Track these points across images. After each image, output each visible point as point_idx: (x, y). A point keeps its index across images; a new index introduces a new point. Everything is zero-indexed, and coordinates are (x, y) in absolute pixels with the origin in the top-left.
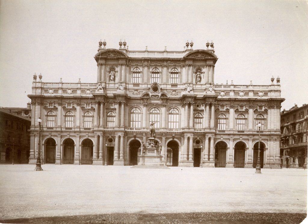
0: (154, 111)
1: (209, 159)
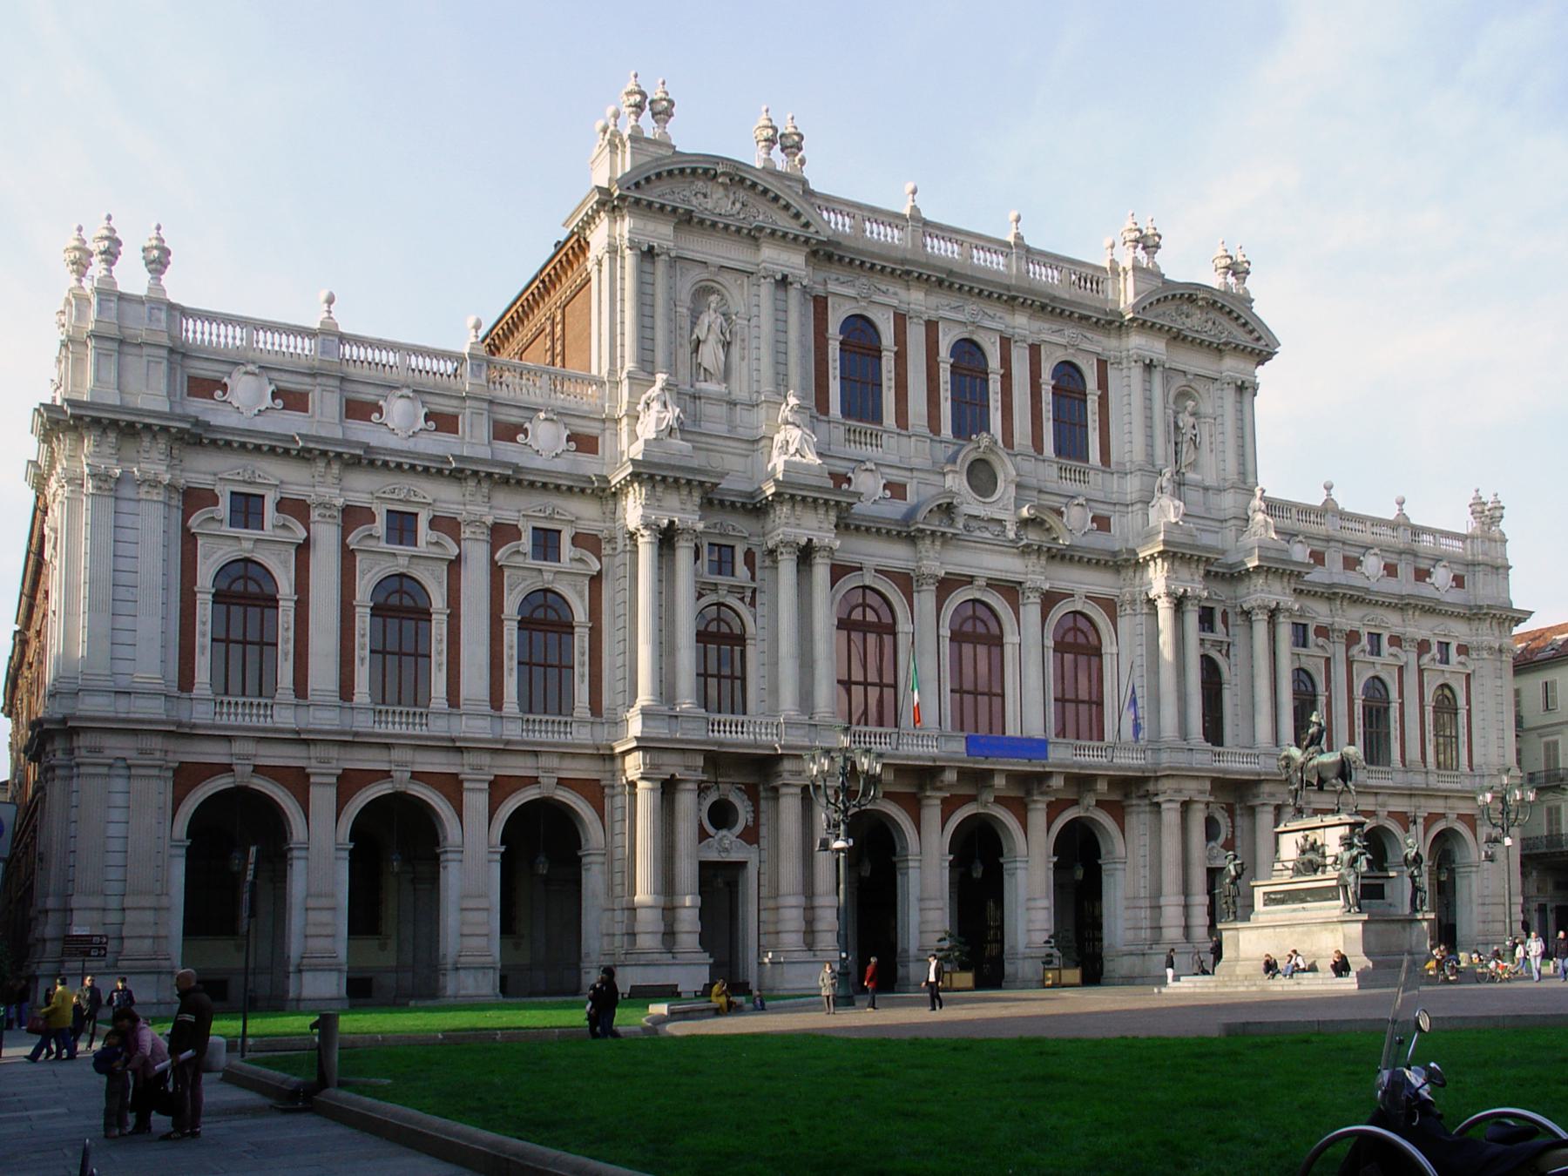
0: (860, 609)
1: (810, 945)
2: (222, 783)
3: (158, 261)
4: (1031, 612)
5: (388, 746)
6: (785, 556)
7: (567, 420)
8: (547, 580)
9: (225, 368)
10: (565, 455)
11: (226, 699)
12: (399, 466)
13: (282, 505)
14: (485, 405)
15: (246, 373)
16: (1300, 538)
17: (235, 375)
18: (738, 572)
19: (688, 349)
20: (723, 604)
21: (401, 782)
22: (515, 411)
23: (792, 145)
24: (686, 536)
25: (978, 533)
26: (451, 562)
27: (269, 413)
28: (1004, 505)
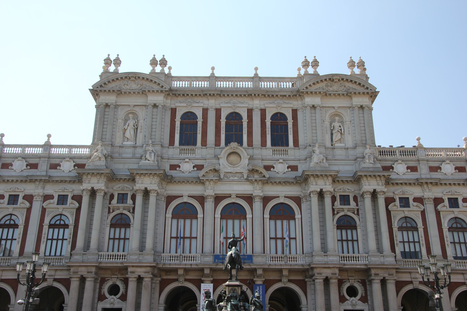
4: (258, 205)
6: (328, 196)
7: (287, 162)
8: (407, 214)
10: (73, 171)
12: (13, 181)
13: (73, 198)
15: (280, 163)
16: (400, 162)
18: (128, 202)
19: (122, 133)
22: (57, 160)
25: (232, 178)
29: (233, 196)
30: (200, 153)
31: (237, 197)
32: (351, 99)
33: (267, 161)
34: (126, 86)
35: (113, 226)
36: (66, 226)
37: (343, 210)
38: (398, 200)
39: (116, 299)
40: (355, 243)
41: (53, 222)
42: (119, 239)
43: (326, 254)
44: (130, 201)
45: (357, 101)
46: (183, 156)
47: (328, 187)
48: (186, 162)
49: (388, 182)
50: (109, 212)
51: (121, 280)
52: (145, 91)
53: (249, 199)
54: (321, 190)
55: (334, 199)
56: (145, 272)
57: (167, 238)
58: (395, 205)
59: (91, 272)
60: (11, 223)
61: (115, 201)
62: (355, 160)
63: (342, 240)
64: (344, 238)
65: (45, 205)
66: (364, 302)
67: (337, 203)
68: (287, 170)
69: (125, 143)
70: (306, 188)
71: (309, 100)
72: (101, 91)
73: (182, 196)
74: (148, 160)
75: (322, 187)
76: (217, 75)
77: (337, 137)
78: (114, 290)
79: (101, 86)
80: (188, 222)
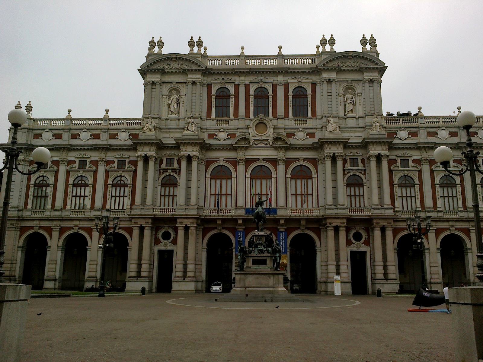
2: (31, 231)
3: (29, 108)
5: (33, 220)
9: (79, 131)
11: (36, 210)
12: (81, 149)
14: (26, 130)
15: (300, 131)
17: (44, 133)
20: (406, 175)
21: (36, 229)
23: (200, 44)
24: (384, 157)
25: (259, 145)
26: (55, 171)
27: (90, 140)
28: (269, 135)
29: (261, 160)
30: (233, 124)
31: (264, 160)
32: (363, 74)
33: (289, 130)
34: (168, 66)
35: (163, 185)
36: (125, 185)
37: (352, 170)
38: (399, 161)
39: (168, 243)
40: (362, 199)
41: (115, 182)
42: (169, 196)
43: (382, 208)
44: (176, 166)
45: (368, 75)
46: (218, 126)
47: (338, 151)
48: (221, 131)
49: (392, 147)
50: (160, 174)
51: (172, 228)
52: (185, 70)
53: (274, 162)
54: (334, 154)
55: (345, 162)
56: (191, 222)
57: (207, 194)
58: (396, 166)
59: (148, 222)
60: (122, 183)
61: (164, 166)
62: (364, 128)
63: (350, 196)
64: (353, 194)
65: (107, 168)
66: (367, 245)
67: (348, 166)
68: (306, 137)
69: (170, 116)
70: (322, 153)
71: (326, 76)
72: (148, 71)
73: (219, 160)
74: (190, 131)
75: (334, 152)
76: (284, 53)
77: (349, 107)
78: (166, 236)
79: (148, 66)
80: (224, 182)
